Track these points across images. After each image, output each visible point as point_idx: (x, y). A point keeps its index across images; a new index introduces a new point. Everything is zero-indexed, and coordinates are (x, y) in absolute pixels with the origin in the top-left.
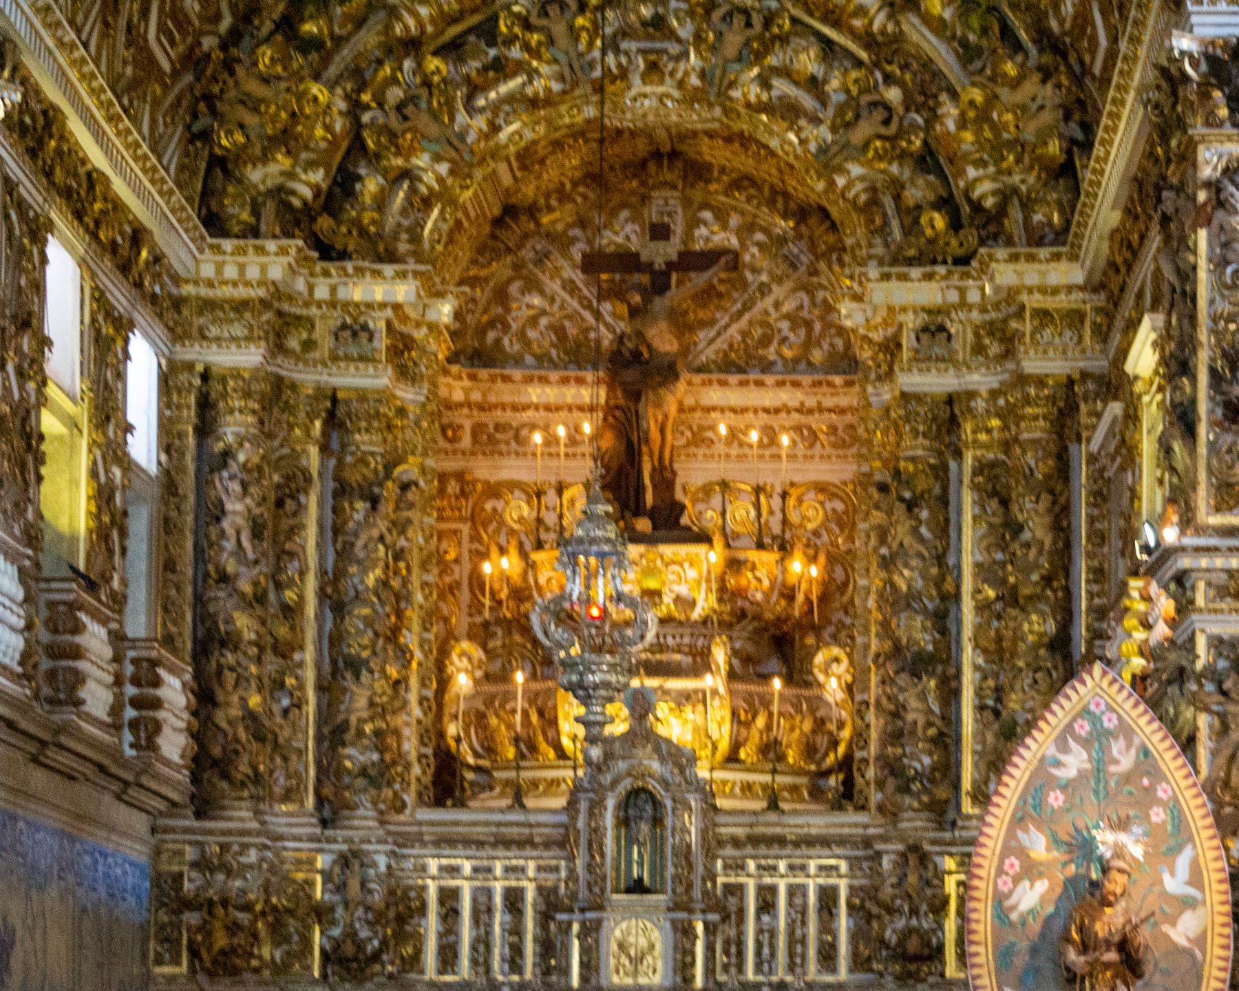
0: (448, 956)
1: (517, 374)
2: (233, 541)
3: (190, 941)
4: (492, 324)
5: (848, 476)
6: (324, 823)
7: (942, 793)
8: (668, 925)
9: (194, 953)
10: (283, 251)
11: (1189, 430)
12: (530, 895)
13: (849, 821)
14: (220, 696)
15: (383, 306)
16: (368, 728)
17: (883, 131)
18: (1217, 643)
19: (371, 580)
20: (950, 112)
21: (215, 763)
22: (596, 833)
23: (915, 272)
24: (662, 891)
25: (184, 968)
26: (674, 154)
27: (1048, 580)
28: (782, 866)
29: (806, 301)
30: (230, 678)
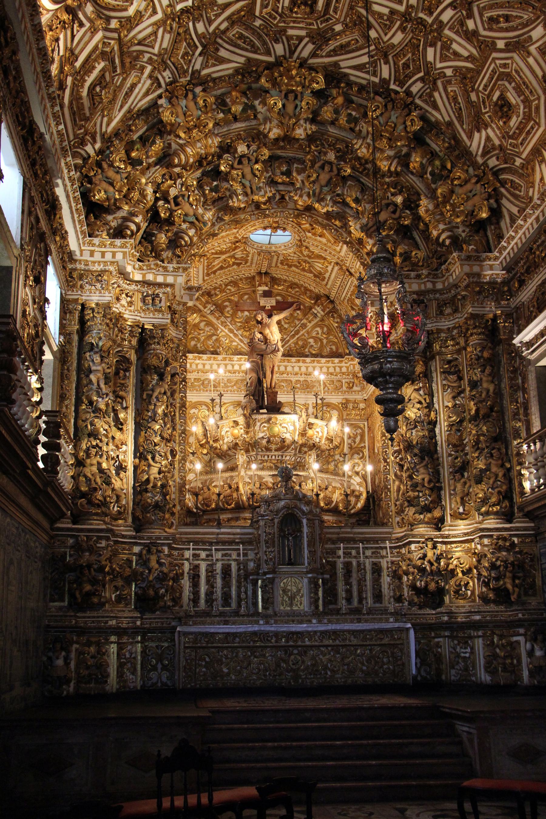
1: (205, 357)
2: (96, 384)
3: (69, 590)
4: (193, 338)
5: (340, 401)
6: (138, 530)
7: (437, 513)
8: (306, 580)
9: (72, 596)
10: (123, 246)
12: (234, 567)
14: (88, 461)
15: (167, 285)
16: (159, 484)
17: (394, 216)
19: (160, 411)
20: (425, 205)
21: (83, 495)
23: (413, 274)
24: (303, 564)
25: (66, 603)
26: (266, 273)
27: (491, 409)
28: (354, 552)
29: (320, 332)
30: (93, 451)
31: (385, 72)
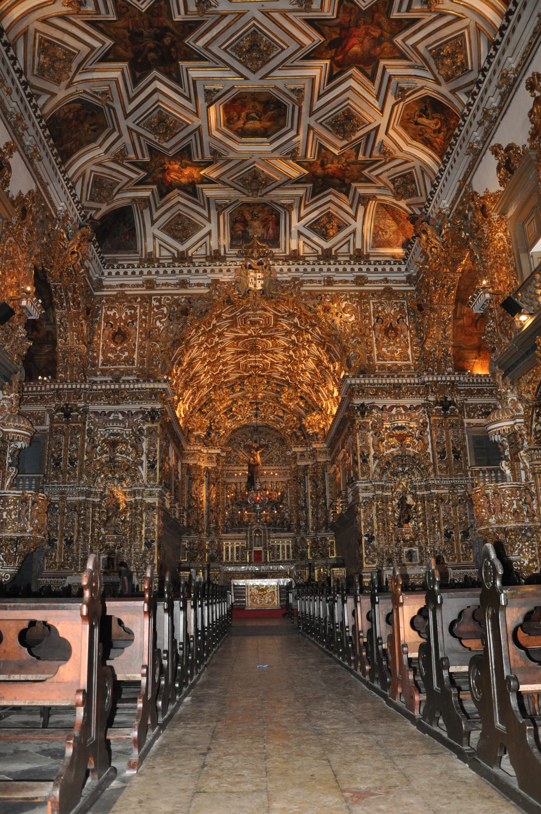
0: (227, 558)
11: (357, 464)
13: (291, 534)
18: (364, 498)
22: (251, 537)
31: (287, 377)
